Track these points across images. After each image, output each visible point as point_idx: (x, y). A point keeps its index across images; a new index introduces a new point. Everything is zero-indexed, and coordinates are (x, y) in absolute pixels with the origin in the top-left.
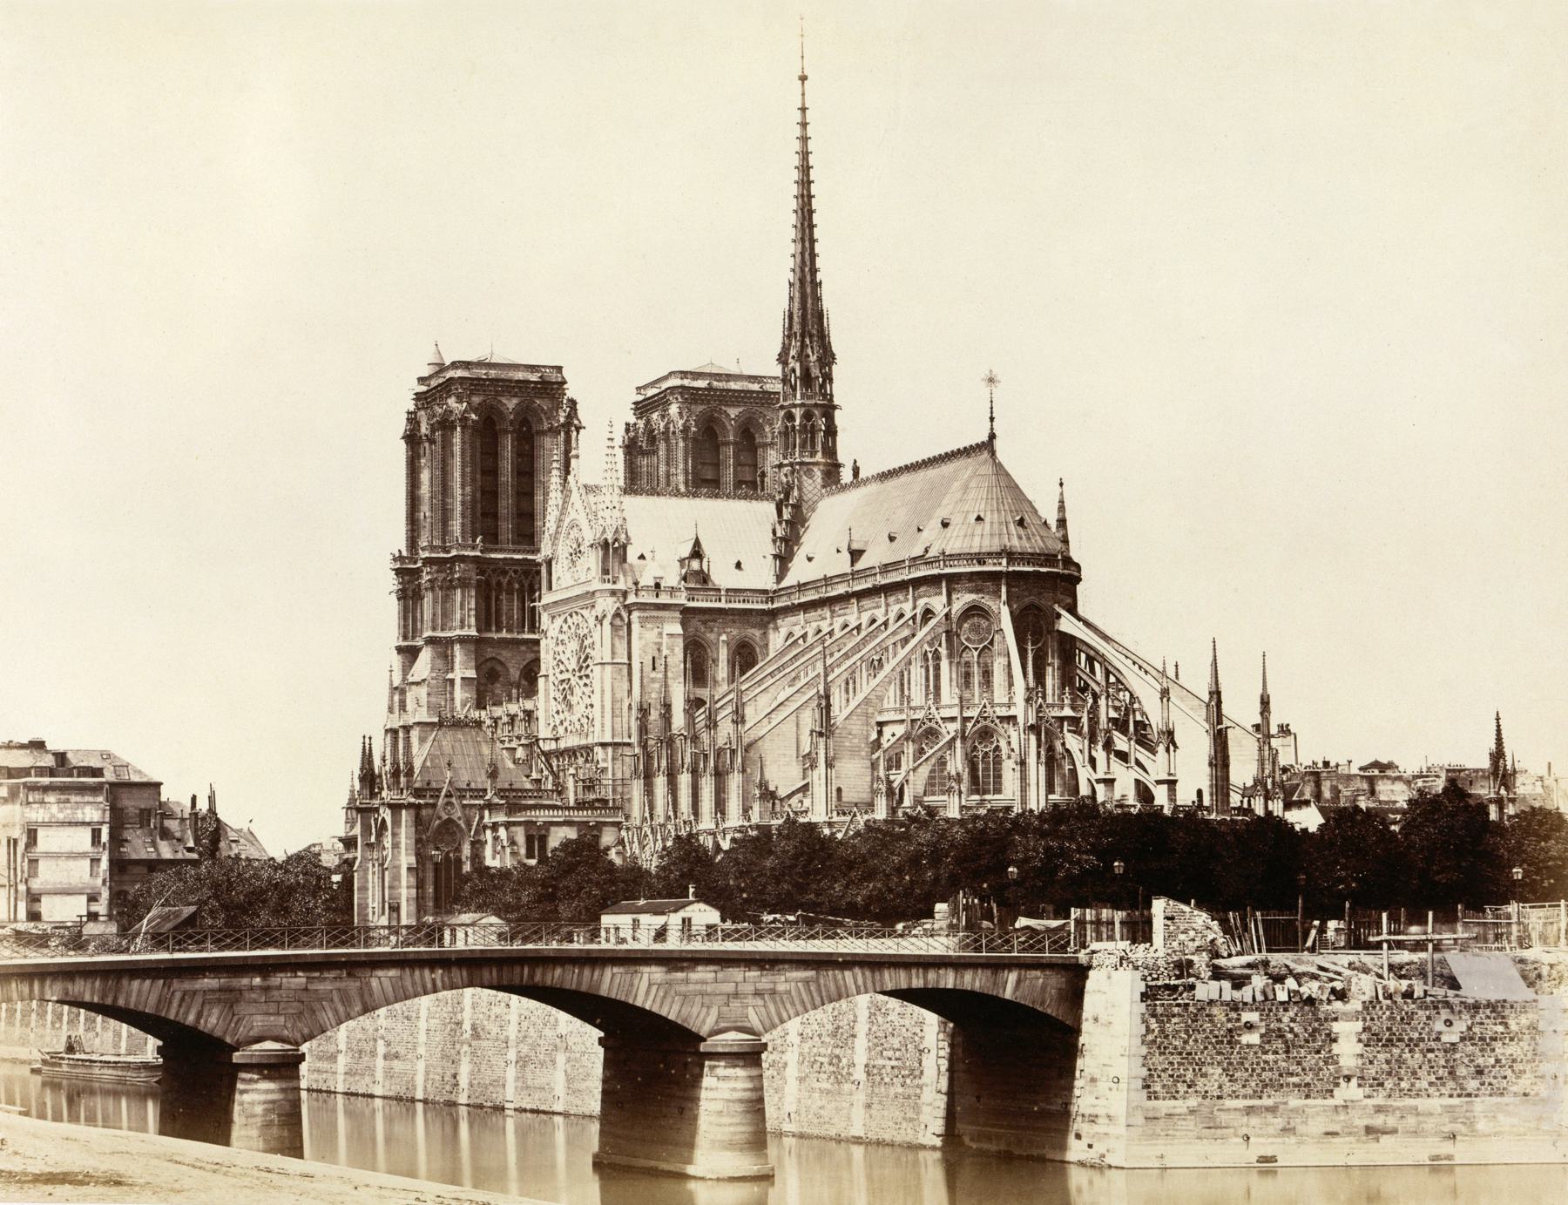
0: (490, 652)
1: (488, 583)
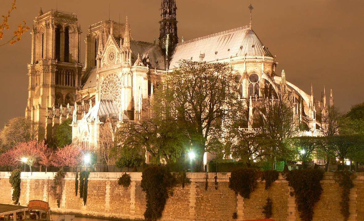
1: (58, 71)
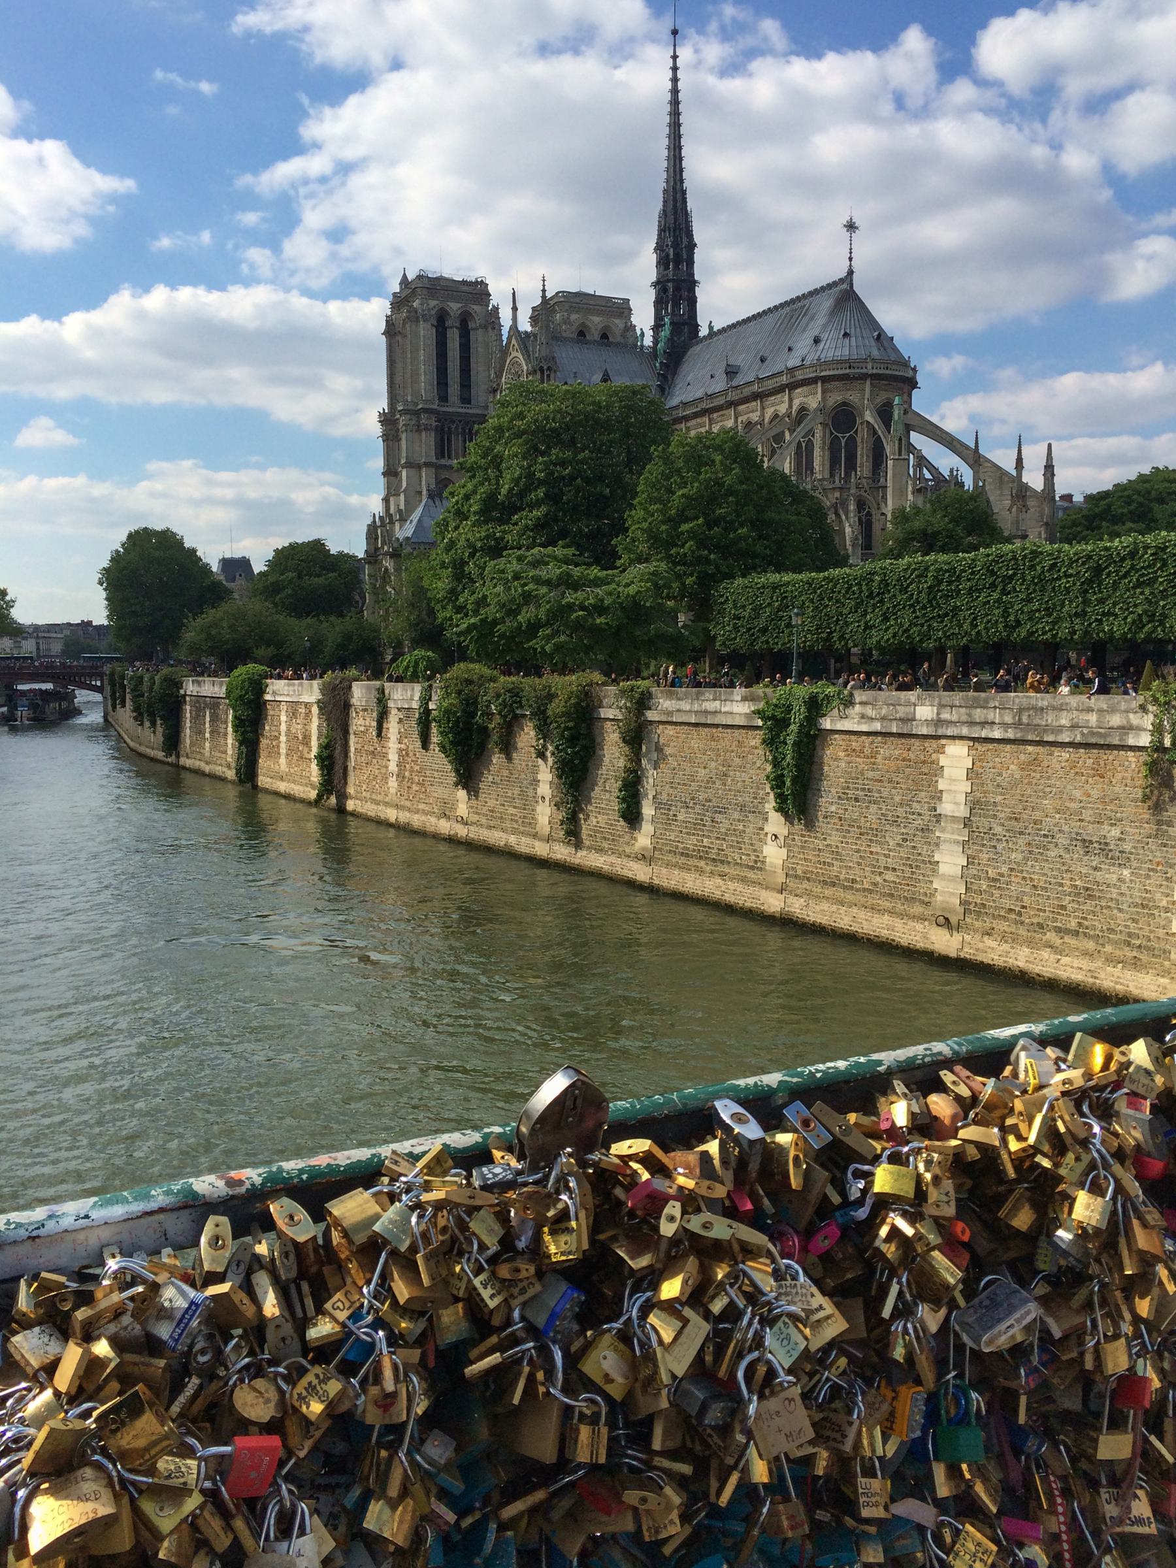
0: (444, 475)
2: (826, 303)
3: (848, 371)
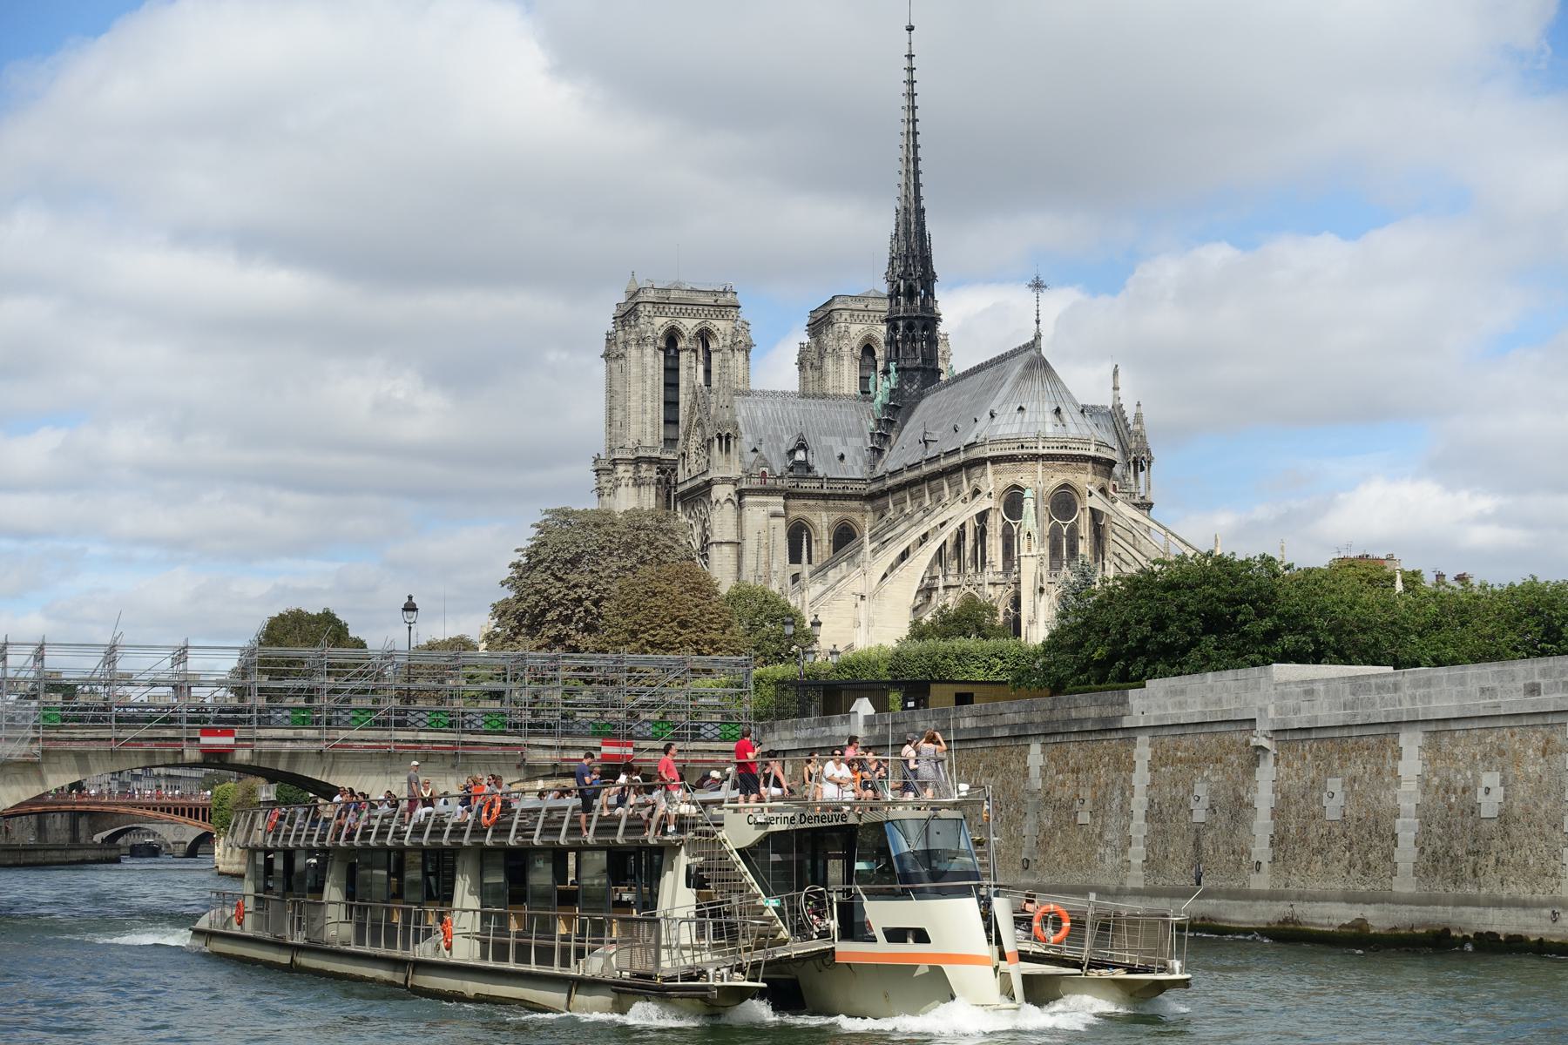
2: (1017, 367)
3: (1015, 452)
